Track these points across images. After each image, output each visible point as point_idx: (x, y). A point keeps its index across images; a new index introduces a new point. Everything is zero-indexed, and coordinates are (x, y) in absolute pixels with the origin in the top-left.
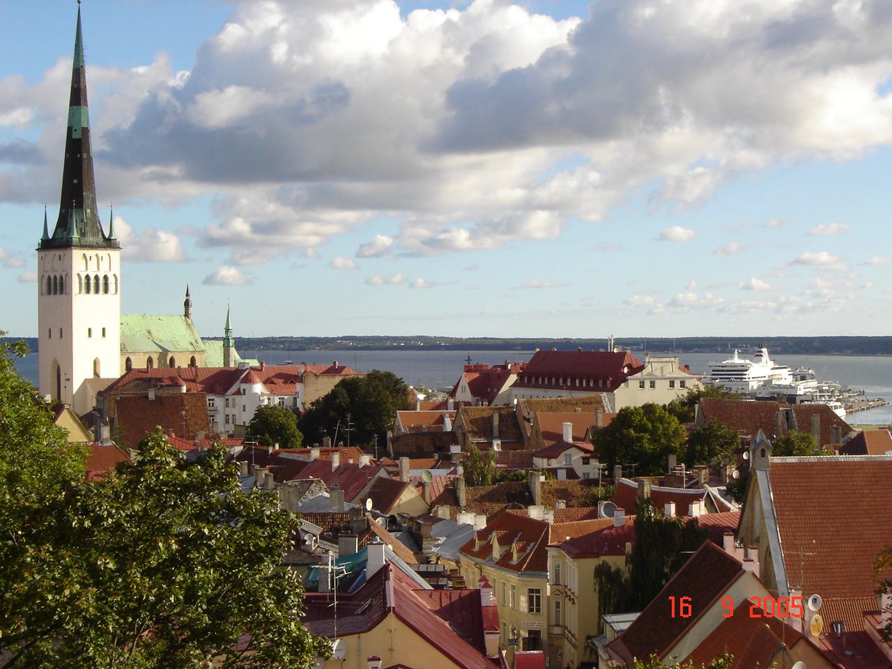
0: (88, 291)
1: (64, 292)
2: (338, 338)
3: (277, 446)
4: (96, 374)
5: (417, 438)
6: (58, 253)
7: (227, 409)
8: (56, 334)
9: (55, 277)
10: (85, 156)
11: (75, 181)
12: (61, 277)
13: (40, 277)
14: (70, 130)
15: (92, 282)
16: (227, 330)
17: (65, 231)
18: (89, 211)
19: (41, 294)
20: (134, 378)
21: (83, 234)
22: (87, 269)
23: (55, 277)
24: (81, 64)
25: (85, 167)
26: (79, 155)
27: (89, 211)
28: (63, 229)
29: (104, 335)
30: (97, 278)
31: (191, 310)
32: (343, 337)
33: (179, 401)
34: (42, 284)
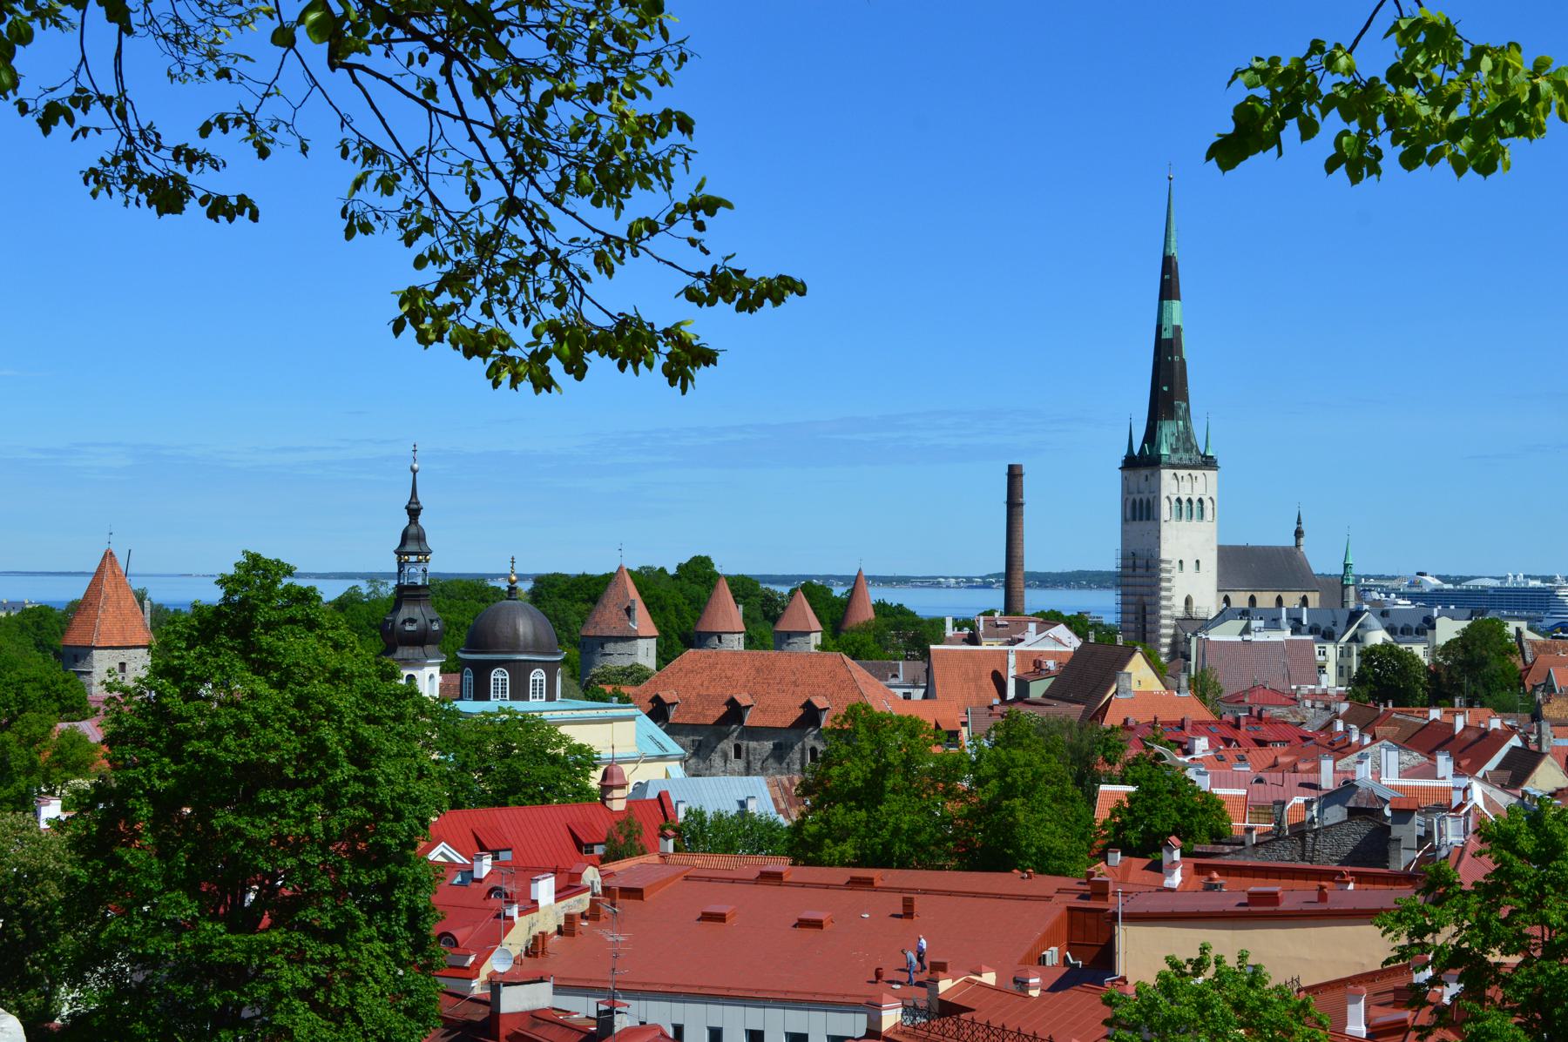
6: (1144, 472)
9: (1141, 500)
10: (1176, 358)
11: (1165, 389)
12: (1148, 501)
15: (1185, 504)
16: (1346, 566)
19: (1125, 520)
21: (1174, 451)
23: (1141, 500)
27: (1181, 423)
30: (1190, 501)
31: (1302, 541)
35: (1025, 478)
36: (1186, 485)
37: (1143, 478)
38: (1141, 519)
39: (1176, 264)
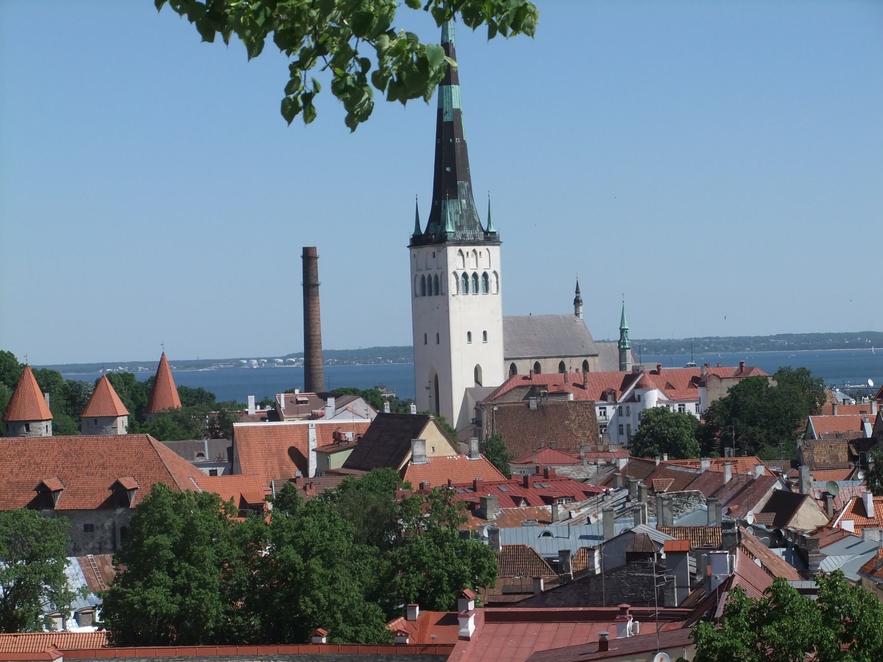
0: (467, 290)
1: (440, 293)
2: (771, 337)
3: (666, 458)
4: (478, 381)
5: (831, 447)
7: (620, 418)
8: (432, 340)
9: (430, 277)
10: (457, 140)
11: (448, 169)
12: (436, 277)
13: (414, 275)
14: (440, 113)
15: (470, 279)
16: (623, 331)
17: (439, 224)
18: (464, 201)
19: (415, 295)
20: (515, 385)
21: (459, 228)
22: (464, 267)
23: (430, 277)
24: (450, 38)
25: (458, 151)
26: (451, 140)
27: (464, 201)
28: (437, 223)
29: (485, 338)
30: (475, 275)
31: (581, 309)
32: (778, 335)
33: (563, 410)
34: (415, 282)
35: (319, 260)
36: (471, 261)
37: (431, 256)
38: (430, 294)
39: (454, 50)
